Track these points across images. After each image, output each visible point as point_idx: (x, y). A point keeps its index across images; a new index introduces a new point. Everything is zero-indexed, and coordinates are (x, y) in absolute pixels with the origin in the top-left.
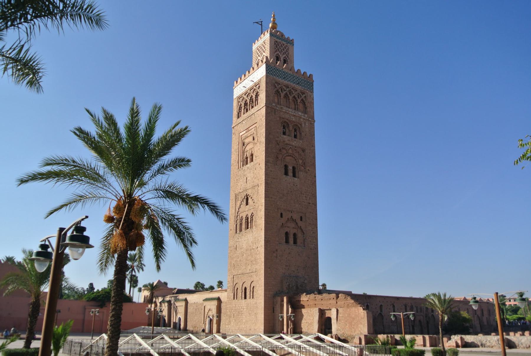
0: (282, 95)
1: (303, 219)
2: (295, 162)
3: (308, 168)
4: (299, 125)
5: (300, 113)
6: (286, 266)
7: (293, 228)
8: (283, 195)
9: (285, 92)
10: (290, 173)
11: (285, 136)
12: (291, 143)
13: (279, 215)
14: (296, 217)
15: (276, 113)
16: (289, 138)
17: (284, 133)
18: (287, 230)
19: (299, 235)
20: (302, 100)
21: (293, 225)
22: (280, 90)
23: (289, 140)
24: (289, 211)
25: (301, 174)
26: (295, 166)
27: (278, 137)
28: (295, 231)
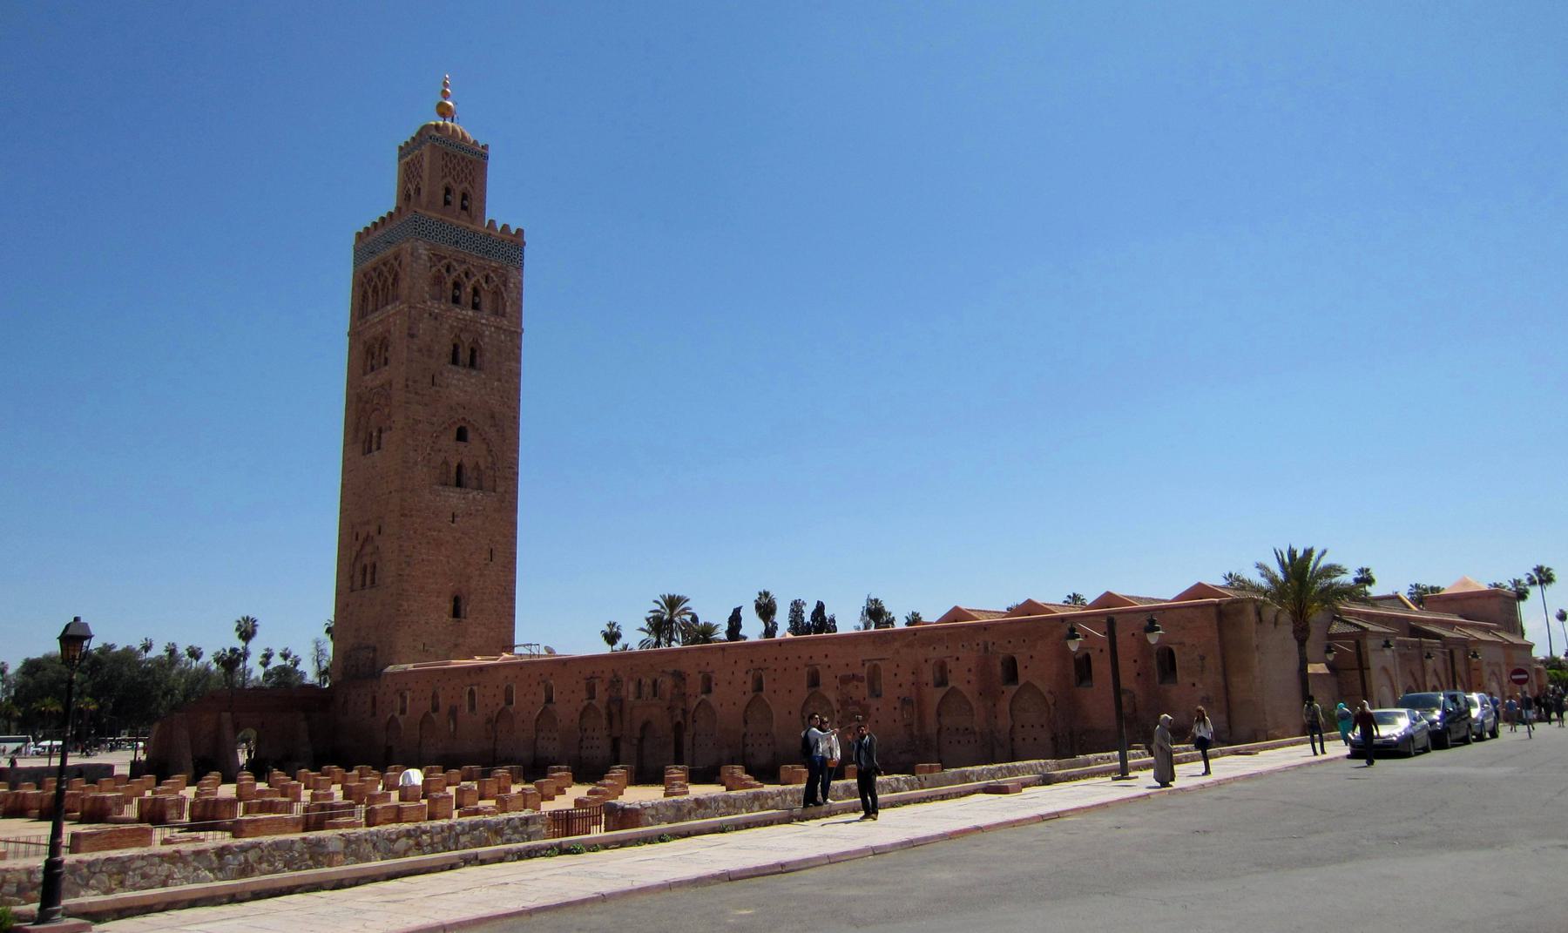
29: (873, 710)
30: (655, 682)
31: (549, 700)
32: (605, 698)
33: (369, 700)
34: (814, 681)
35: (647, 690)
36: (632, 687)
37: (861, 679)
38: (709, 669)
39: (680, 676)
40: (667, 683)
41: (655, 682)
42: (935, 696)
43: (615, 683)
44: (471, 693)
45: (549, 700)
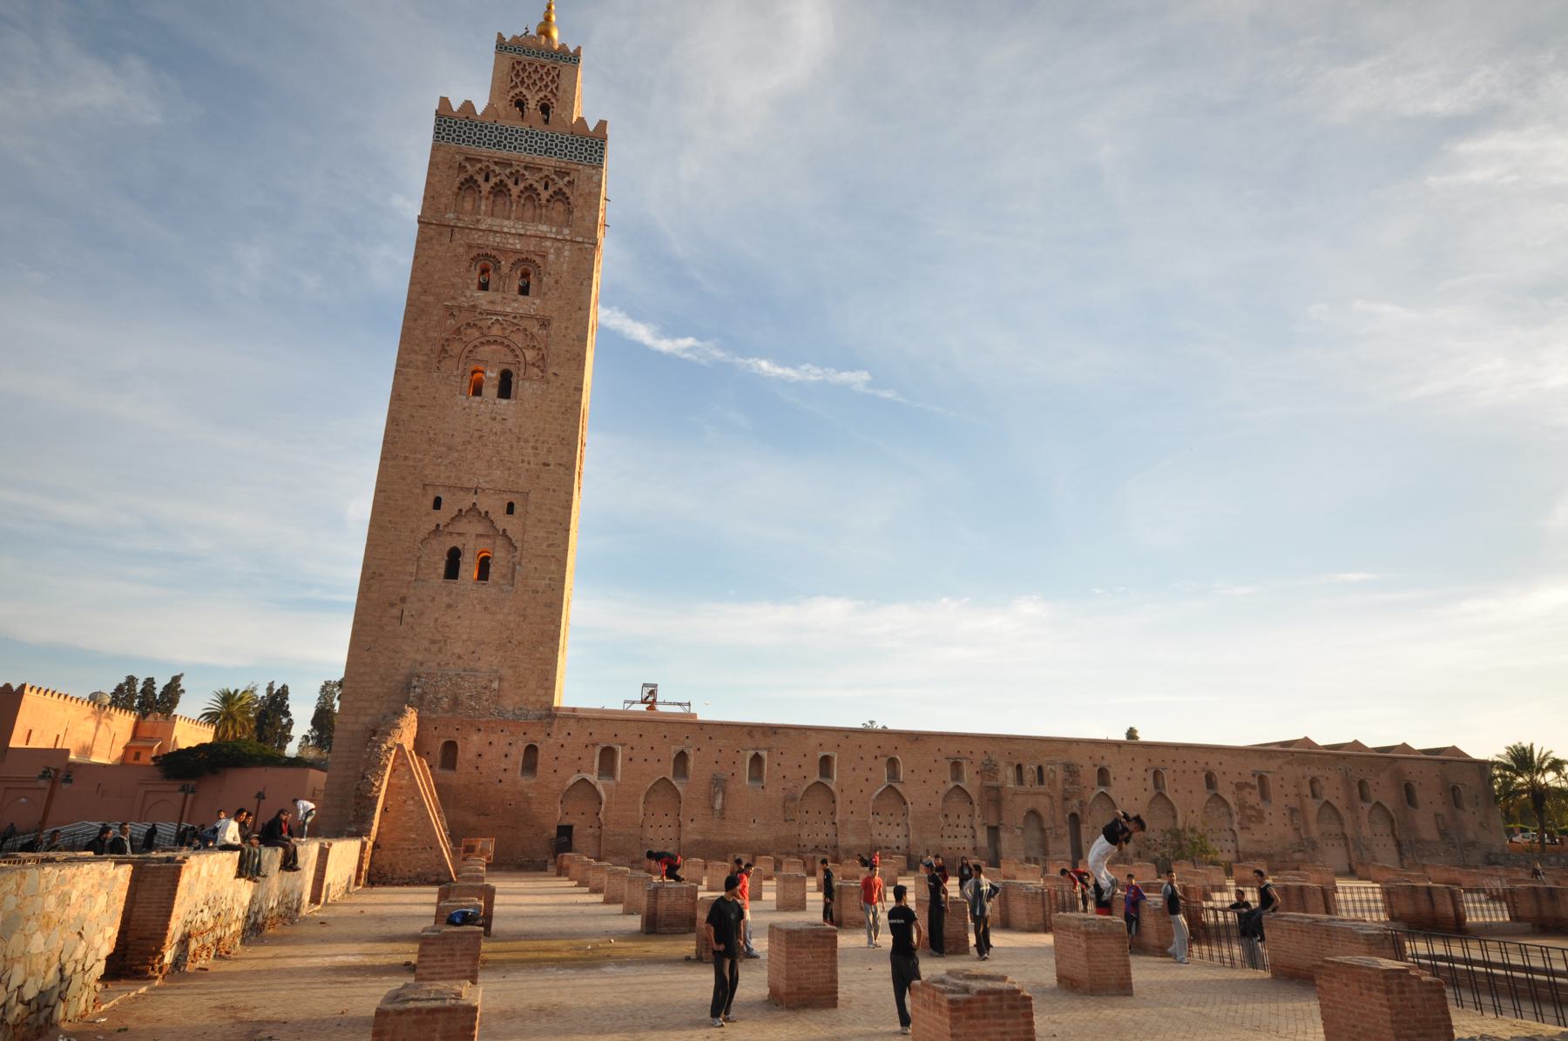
0: (486, 188)
1: (518, 509)
2: (510, 358)
3: (551, 370)
4: (538, 260)
5: (544, 228)
6: (433, 642)
7: (478, 536)
8: (450, 448)
9: (493, 180)
10: (490, 390)
11: (481, 294)
12: (499, 308)
13: (430, 502)
14: (492, 504)
15: (457, 236)
16: (498, 297)
17: (484, 287)
18: (456, 542)
19: (499, 556)
20: (559, 192)
21: (480, 528)
22: (480, 179)
23: (492, 302)
24: (468, 490)
25: (524, 388)
26: (512, 368)
27: (453, 298)
28: (484, 544)
29: (1266, 815)
30: (1040, 768)
31: (893, 775)
32: (978, 782)
33: (517, 754)
34: (1210, 781)
35: (1029, 777)
36: (1010, 773)
37: (1253, 787)
38: (1104, 763)
39: (1071, 771)
40: (1056, 773)
41: (1040, 768)
42: (1313, 807)
43: (989, 769)
44: (757, 759)
45: (893, 775)
